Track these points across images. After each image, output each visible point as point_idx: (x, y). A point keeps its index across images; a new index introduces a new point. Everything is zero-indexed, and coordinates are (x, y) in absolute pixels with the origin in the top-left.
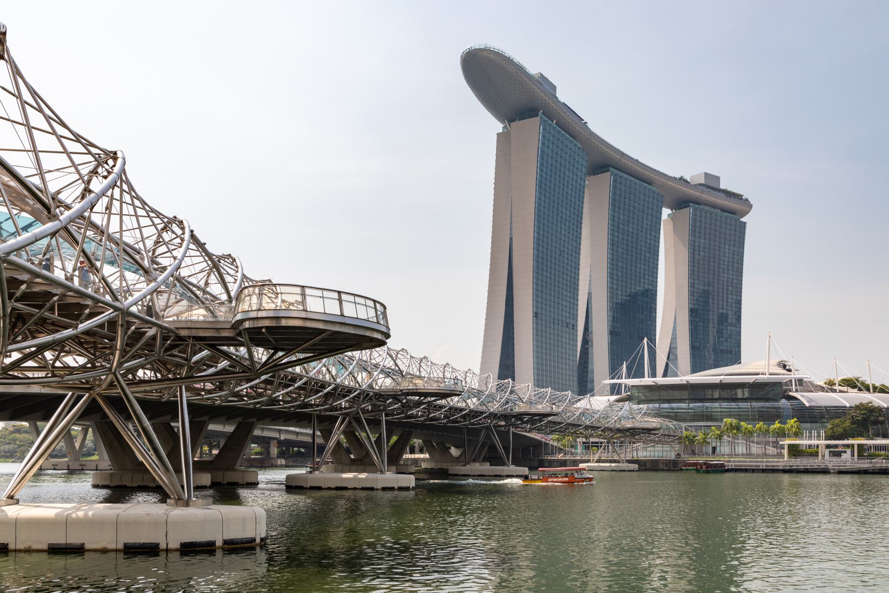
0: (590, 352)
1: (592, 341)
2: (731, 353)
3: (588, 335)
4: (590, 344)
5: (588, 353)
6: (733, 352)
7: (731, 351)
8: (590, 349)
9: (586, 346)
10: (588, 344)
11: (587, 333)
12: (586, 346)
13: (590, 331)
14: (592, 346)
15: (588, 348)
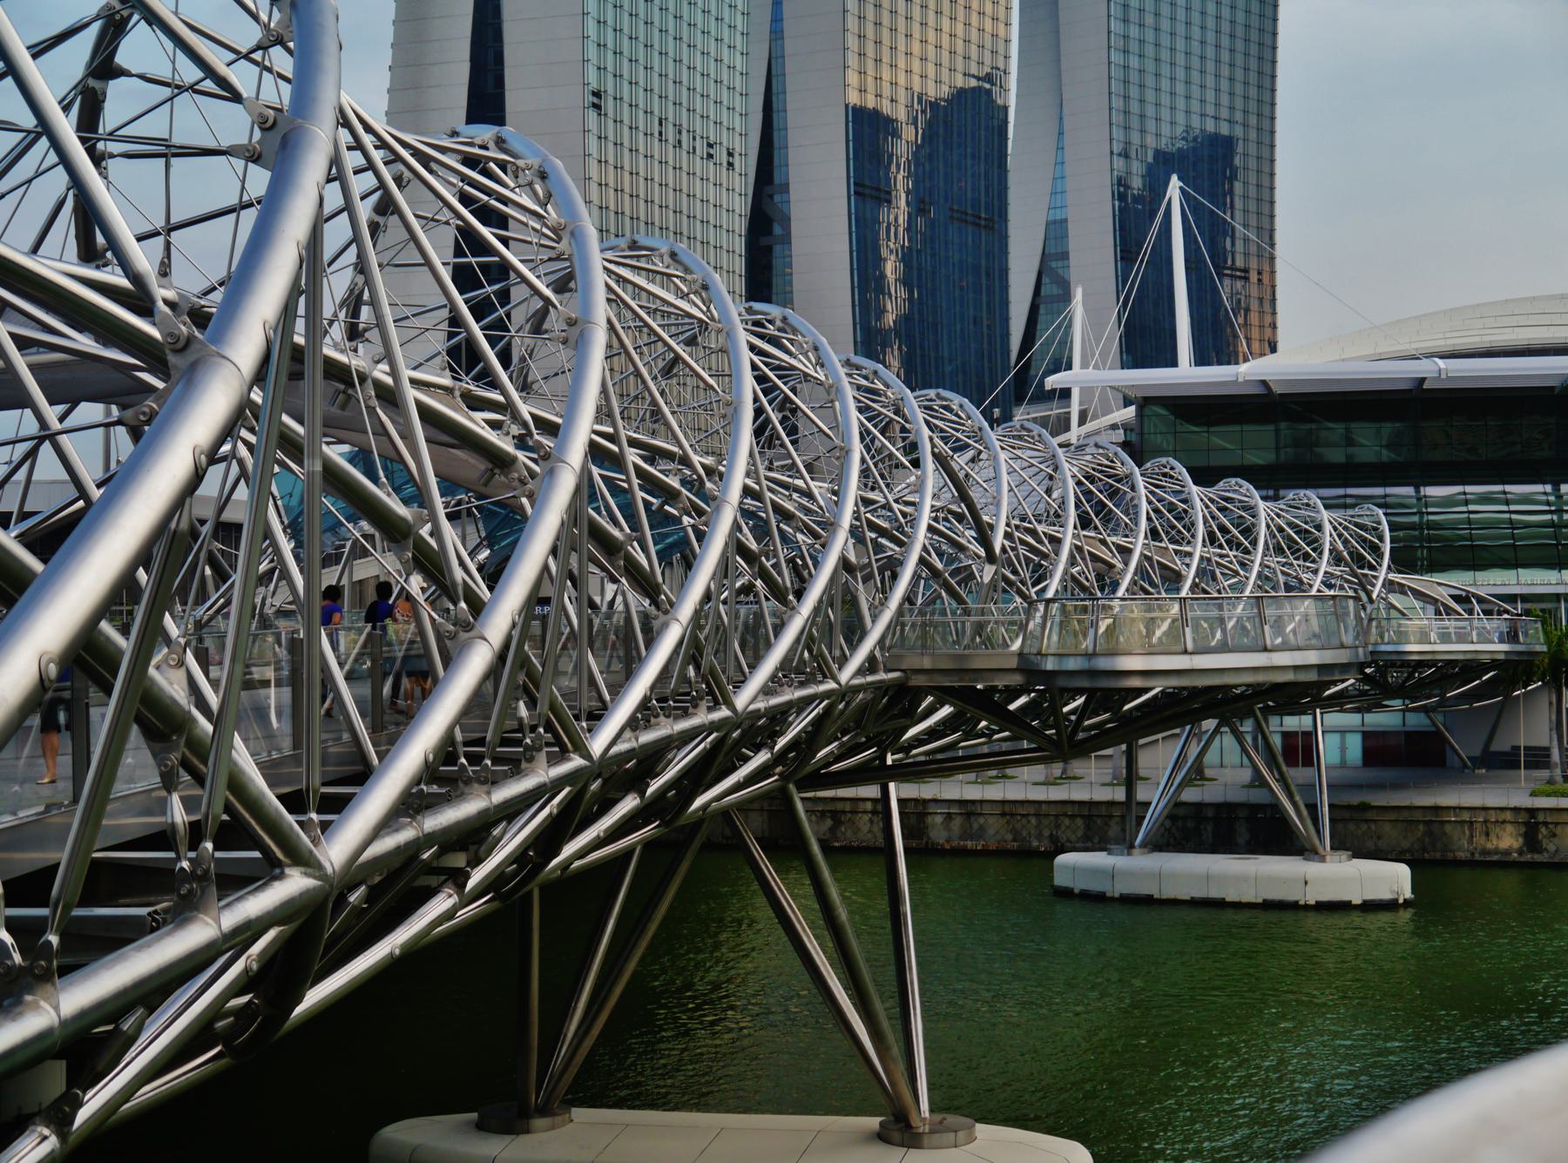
0: (777, 263)
1: (786, 221)
2: (1246, 279)
3: (771, 197)
4: (777, 230)
5: (769, 267)
6: (1254, 277)
7: (1246, 271)
8: (777, 249)
9: (764, 241)
10: (769, 232)
11: (768, 190)
12: (764, 241)
13: (777, 180)
14: (786, 239)
15: (769, 250)
